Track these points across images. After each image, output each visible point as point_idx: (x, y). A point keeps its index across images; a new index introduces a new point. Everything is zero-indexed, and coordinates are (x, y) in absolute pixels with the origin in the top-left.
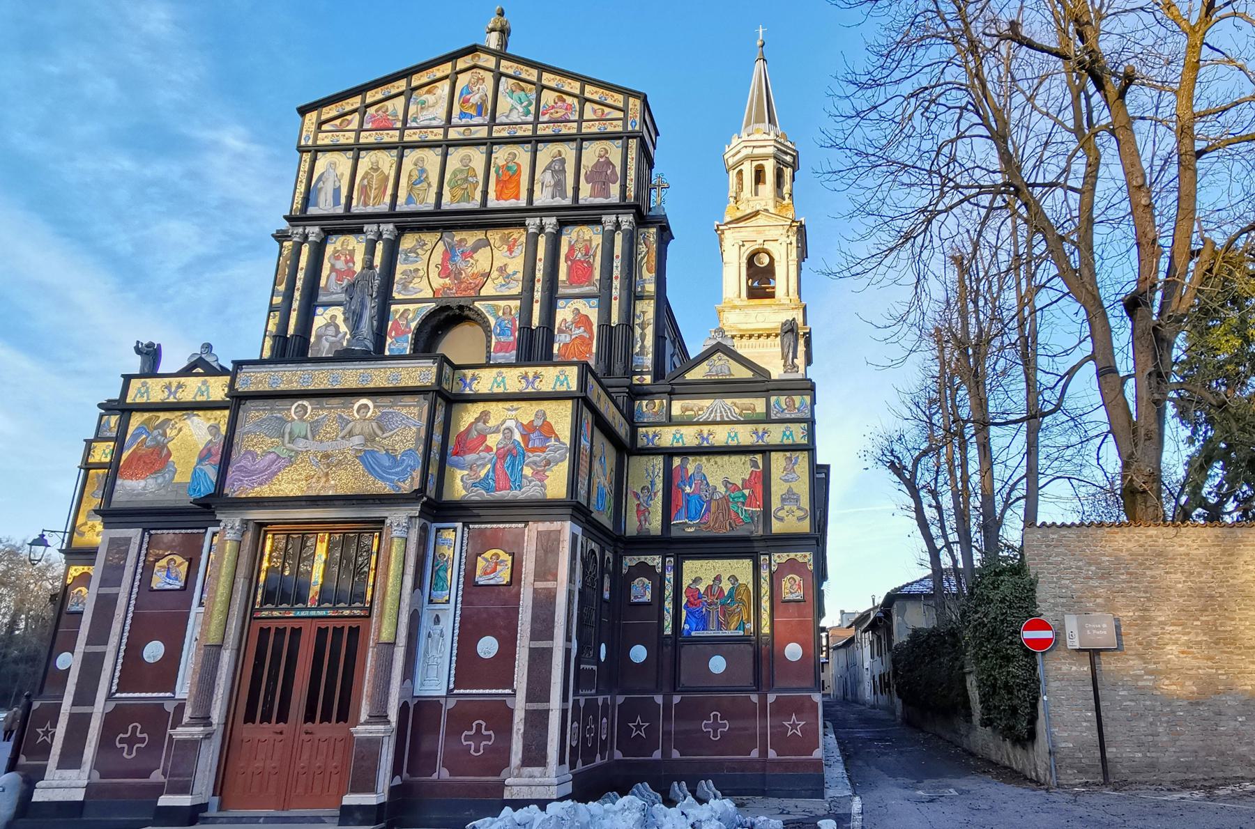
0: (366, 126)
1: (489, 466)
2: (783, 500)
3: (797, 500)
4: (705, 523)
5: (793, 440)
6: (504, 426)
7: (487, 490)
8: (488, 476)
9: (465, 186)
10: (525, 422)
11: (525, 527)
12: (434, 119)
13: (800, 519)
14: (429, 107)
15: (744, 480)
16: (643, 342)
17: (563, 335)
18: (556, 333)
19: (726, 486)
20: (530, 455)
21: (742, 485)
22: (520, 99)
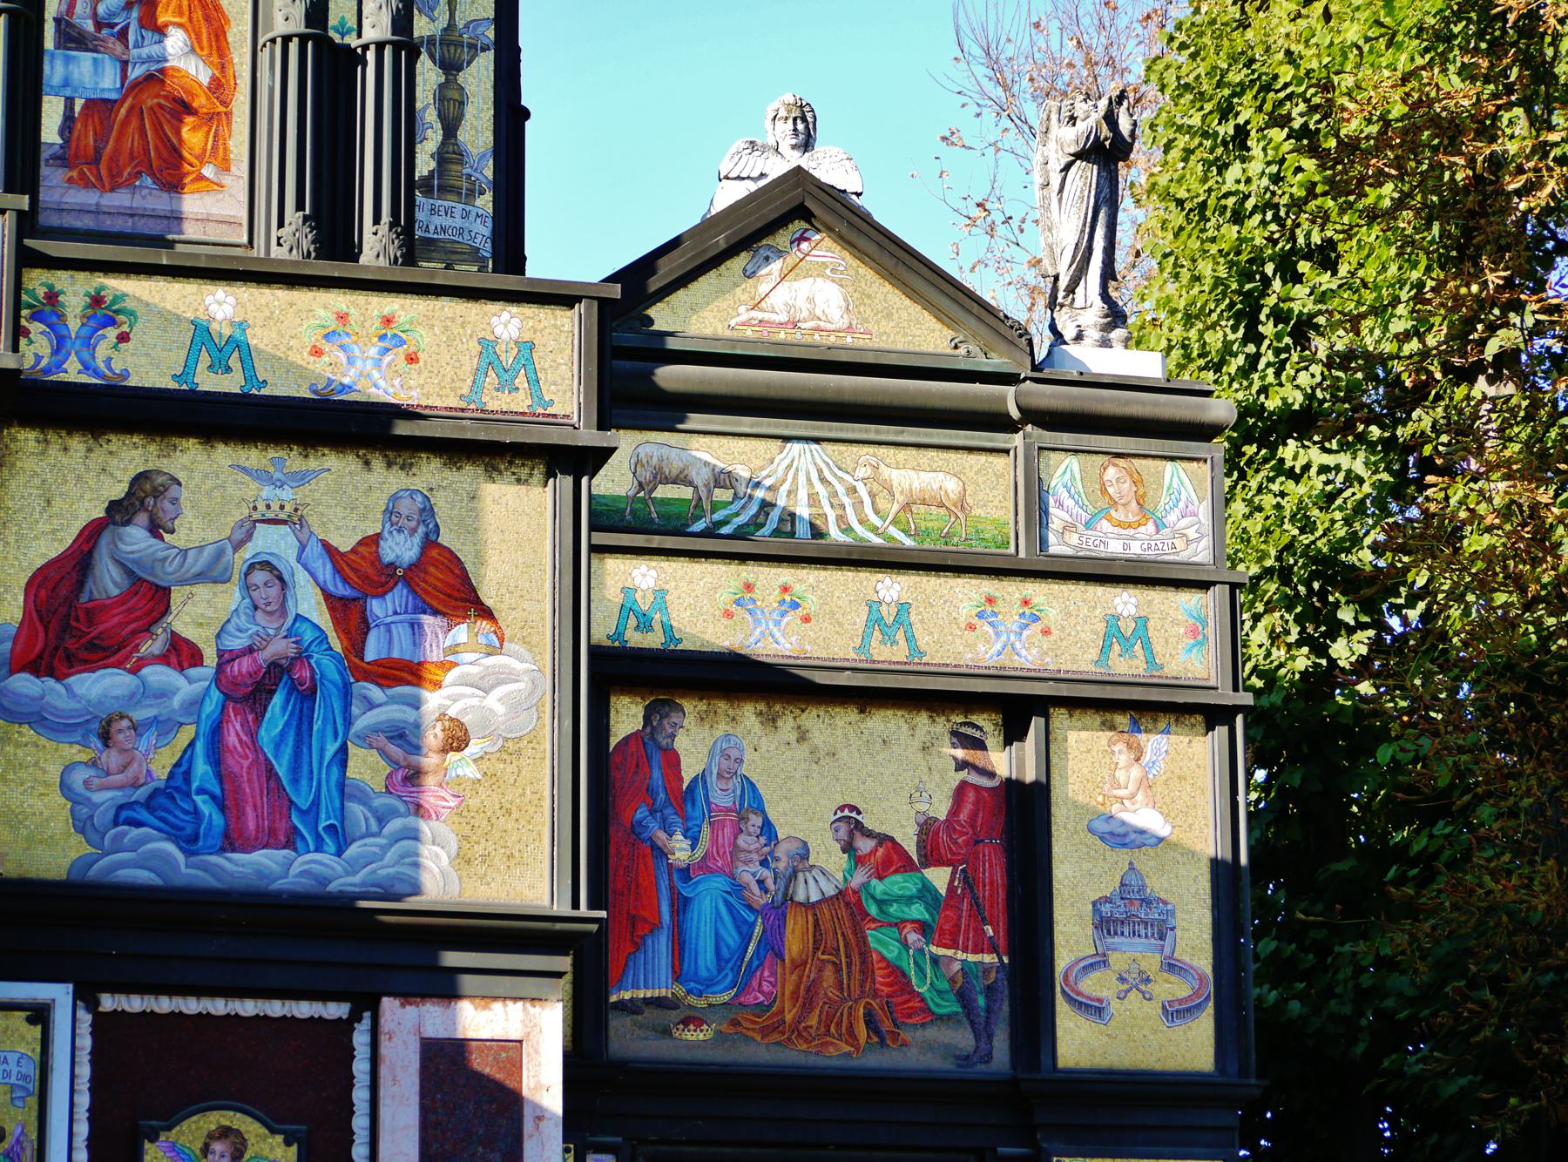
1: (185, 735)
2: (1105, 924)
3: (1163, 931)
4: (761, 1009)
5: (1150, 658)
6: (247, 552)
7: (189, 842)
8: (187, 776)
10: (345, 543)
11: (355, 1017)
13: (1176, 1012)
15: (928, 830)
16: (450, 127)
17: (86, 58)
18: (49, 43)
19: (848, 847)
20: (375, 692)
21: (920, 845)
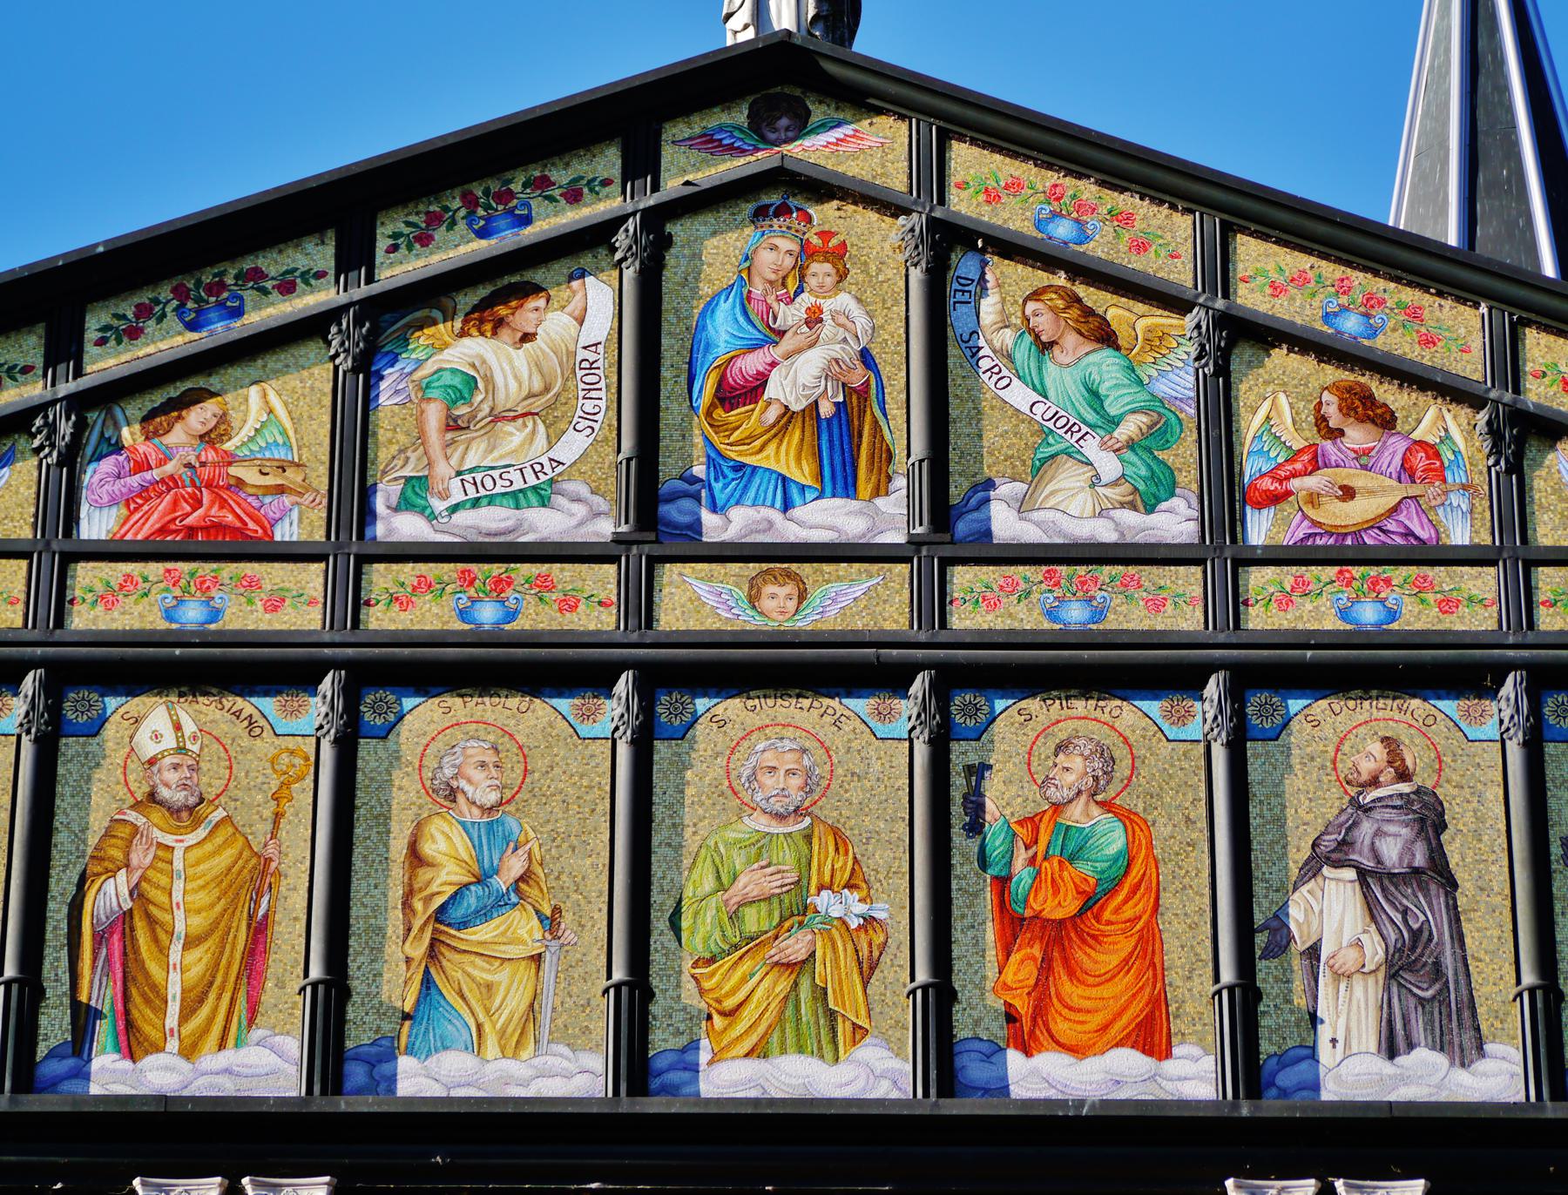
0: (96, 525)
9: (795, 946)
12: (543, 495)
14: (497, 418)
22: (1094, 396)
